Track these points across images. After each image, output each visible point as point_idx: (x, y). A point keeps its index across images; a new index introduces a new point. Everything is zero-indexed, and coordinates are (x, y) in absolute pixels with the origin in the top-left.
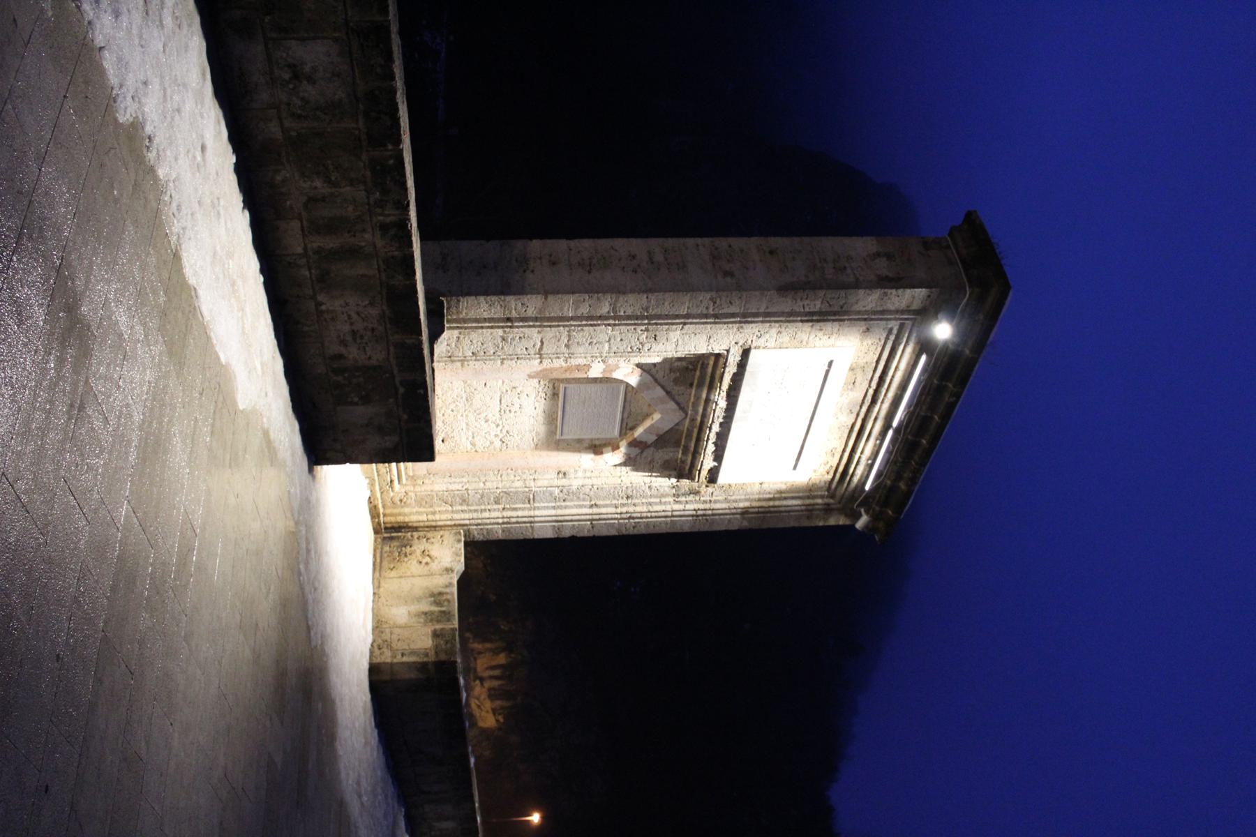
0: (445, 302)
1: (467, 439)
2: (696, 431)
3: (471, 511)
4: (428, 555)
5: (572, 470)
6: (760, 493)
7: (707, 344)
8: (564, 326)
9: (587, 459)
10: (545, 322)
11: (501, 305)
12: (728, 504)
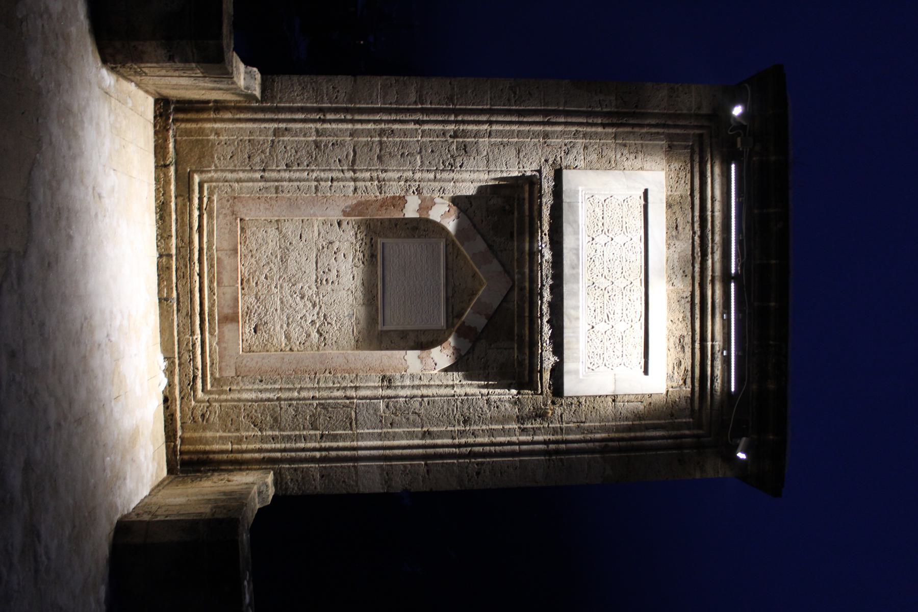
1: (282, 327)
2: (527, 305)
3: (283, 437)
5: (398, 375)
6: (615, 419)
7: (518, 160)
9: (412, 356)
11: (313, 88)
12: (582, 436)
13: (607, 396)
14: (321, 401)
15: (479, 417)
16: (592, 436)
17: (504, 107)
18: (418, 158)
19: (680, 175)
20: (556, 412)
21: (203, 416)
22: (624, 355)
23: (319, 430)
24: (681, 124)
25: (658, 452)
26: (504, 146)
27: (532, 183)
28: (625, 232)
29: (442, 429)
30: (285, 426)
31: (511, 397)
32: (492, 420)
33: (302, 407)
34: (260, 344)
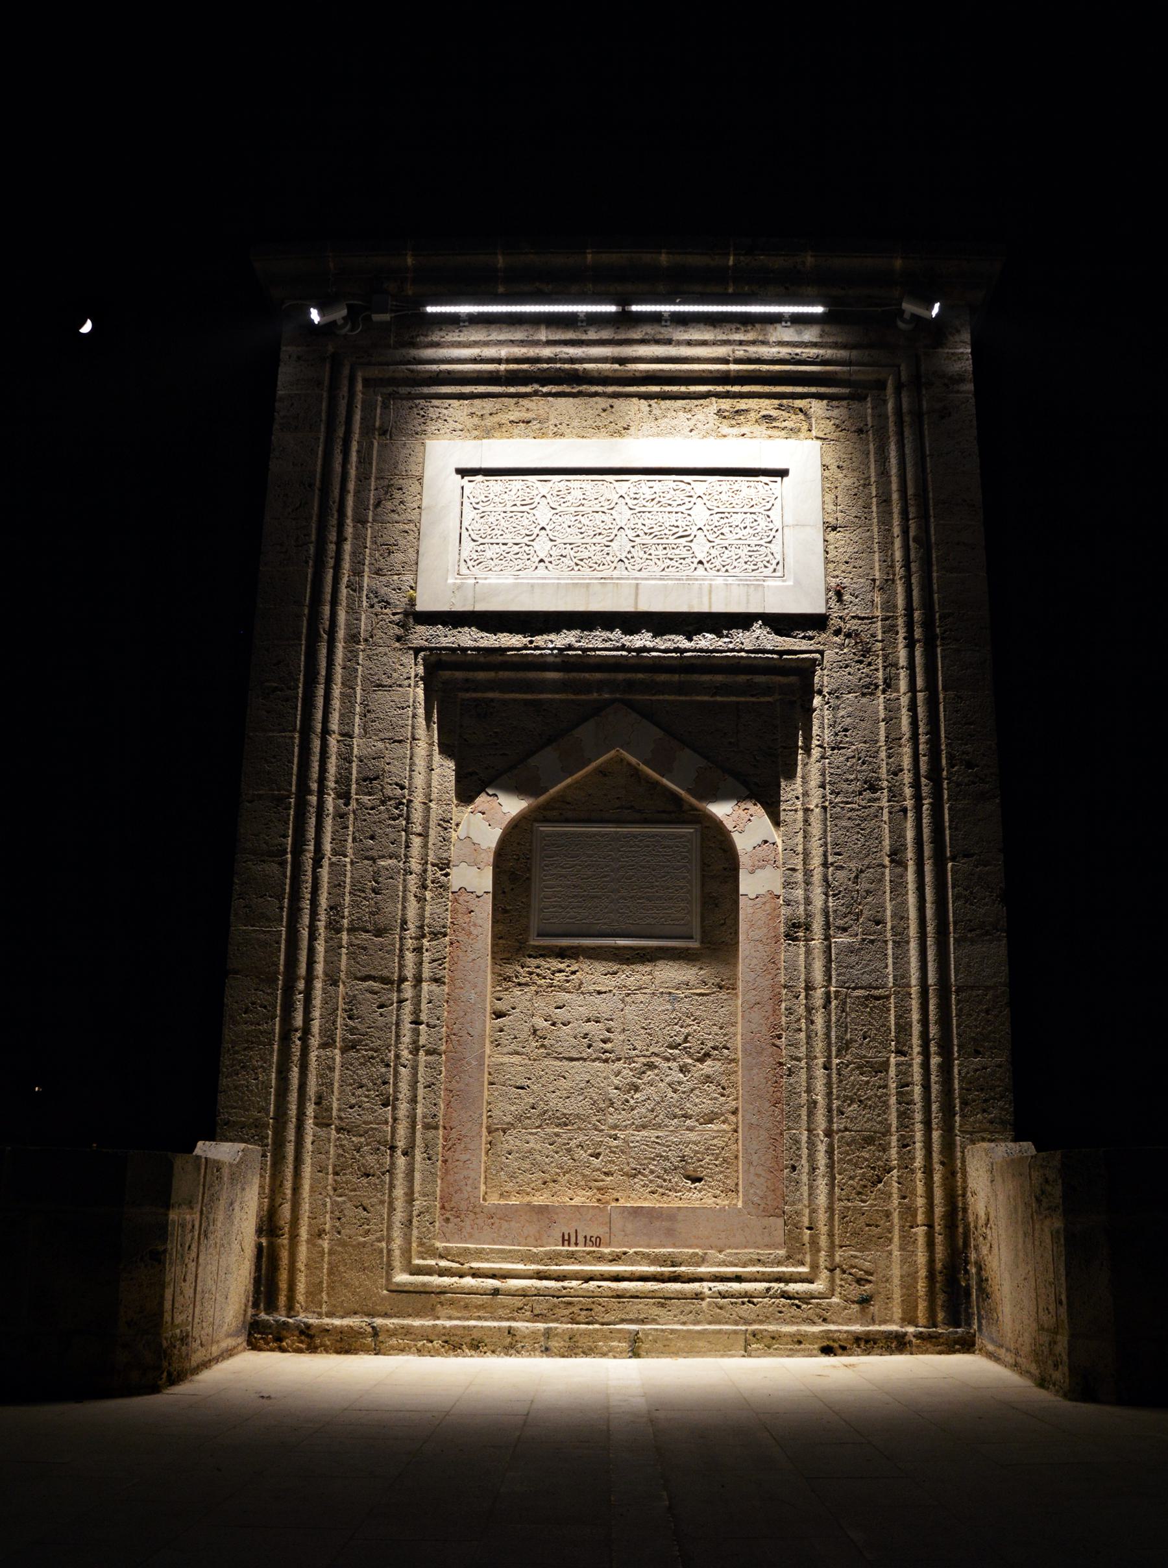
3: (902, 1126)
9: (751, 885)
11: (245, 1049)
12: (898, 582)
13: (825, 541)
15: (864, 763)
16: (898, 565)
17: (299, 708)
18: (383, 863)
19: (434, 417)
20: (856, 628)
21: (859, 1281)
22: (752, 510)
23: (888, 1058)
24: (344, 412)
25: (928, 453)
26: (369, 711)
29: (887, 831)
30: (880, 1122)
31: (827, 706)
33: (845, 1089)
34: (721, 1172)
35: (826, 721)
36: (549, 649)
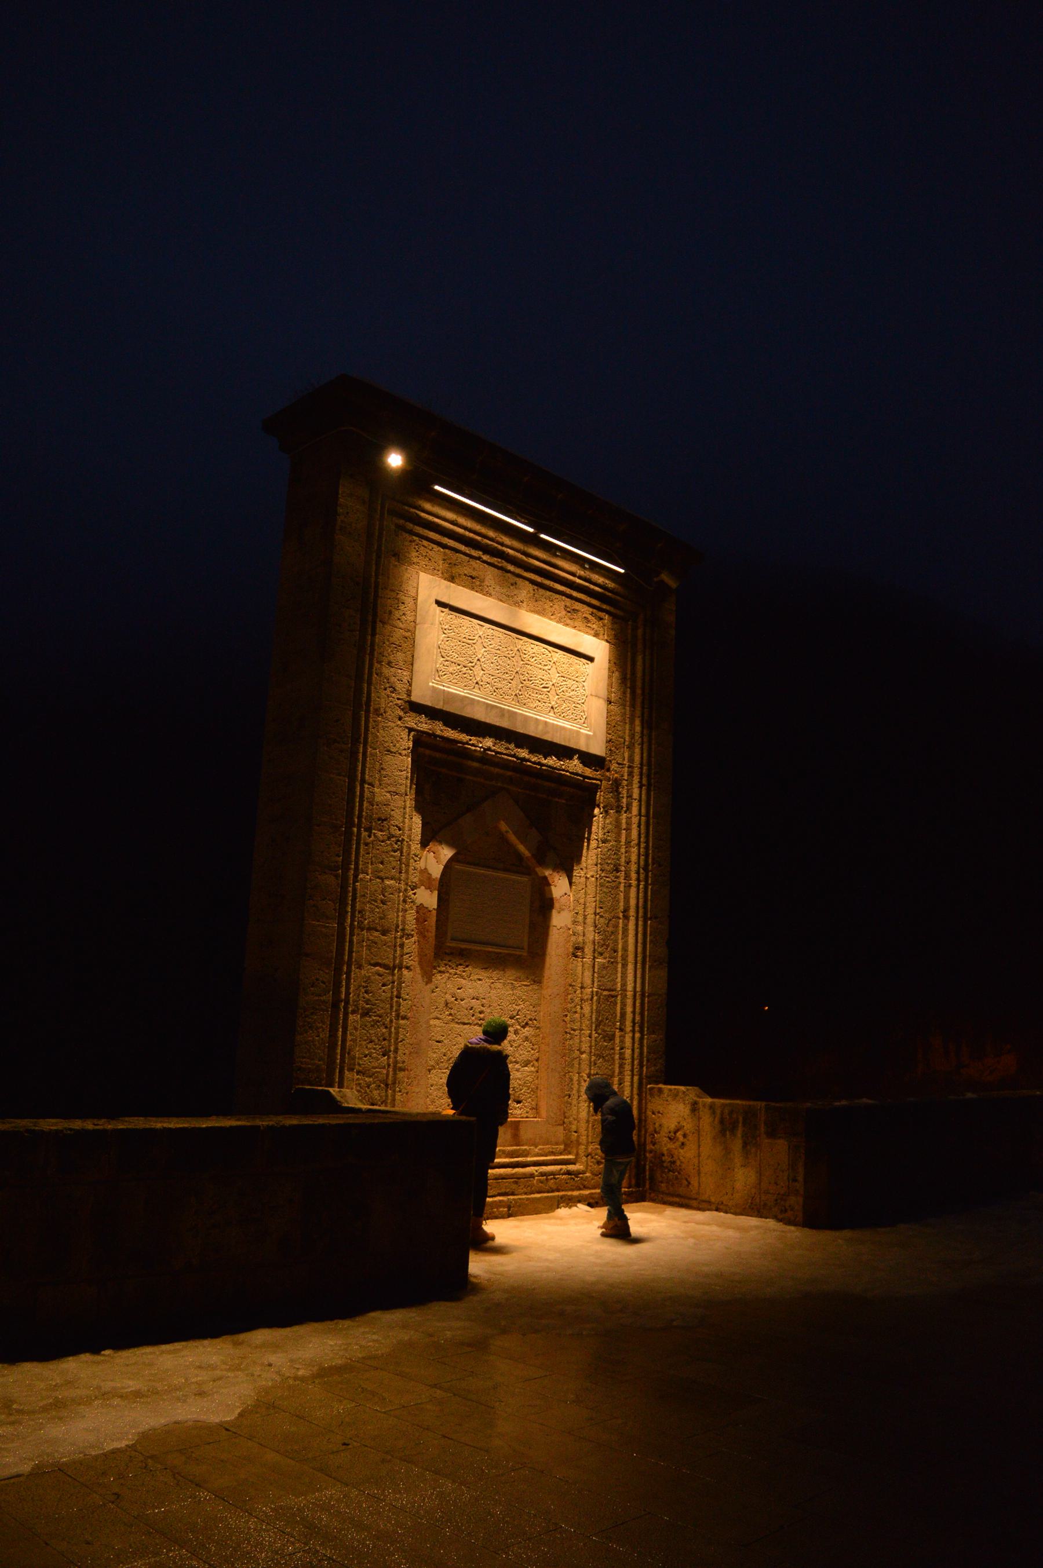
0: (297, 1087)
3: (620, 1073)
4: (675, 1133)
5: (573, 938)
6: (624, 706)
7: (397, 755)
8: (352, 934)
9: (559, 920)
10: (343, 958)
11: (312, 1014)
12: (636, 745)
14: (594, 1028)
18: (388, 883)
22: (577, 679)
23: (615, 1032)
26: (382, 769)
27: (421, 741)
28: (474, 641)
30: (610, 1070)
31: (601, 815)
32: (618, 841)
34: (530, 1097)
35: (600, 825)
36: (479, 747)
